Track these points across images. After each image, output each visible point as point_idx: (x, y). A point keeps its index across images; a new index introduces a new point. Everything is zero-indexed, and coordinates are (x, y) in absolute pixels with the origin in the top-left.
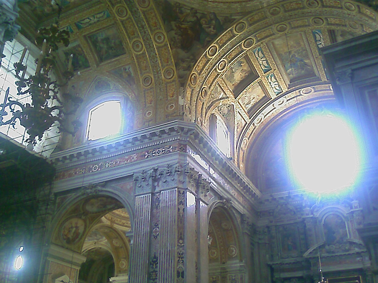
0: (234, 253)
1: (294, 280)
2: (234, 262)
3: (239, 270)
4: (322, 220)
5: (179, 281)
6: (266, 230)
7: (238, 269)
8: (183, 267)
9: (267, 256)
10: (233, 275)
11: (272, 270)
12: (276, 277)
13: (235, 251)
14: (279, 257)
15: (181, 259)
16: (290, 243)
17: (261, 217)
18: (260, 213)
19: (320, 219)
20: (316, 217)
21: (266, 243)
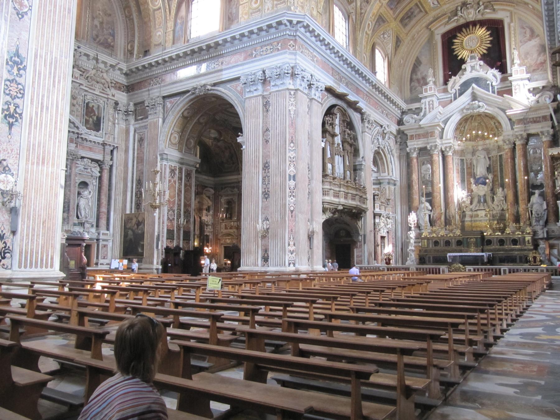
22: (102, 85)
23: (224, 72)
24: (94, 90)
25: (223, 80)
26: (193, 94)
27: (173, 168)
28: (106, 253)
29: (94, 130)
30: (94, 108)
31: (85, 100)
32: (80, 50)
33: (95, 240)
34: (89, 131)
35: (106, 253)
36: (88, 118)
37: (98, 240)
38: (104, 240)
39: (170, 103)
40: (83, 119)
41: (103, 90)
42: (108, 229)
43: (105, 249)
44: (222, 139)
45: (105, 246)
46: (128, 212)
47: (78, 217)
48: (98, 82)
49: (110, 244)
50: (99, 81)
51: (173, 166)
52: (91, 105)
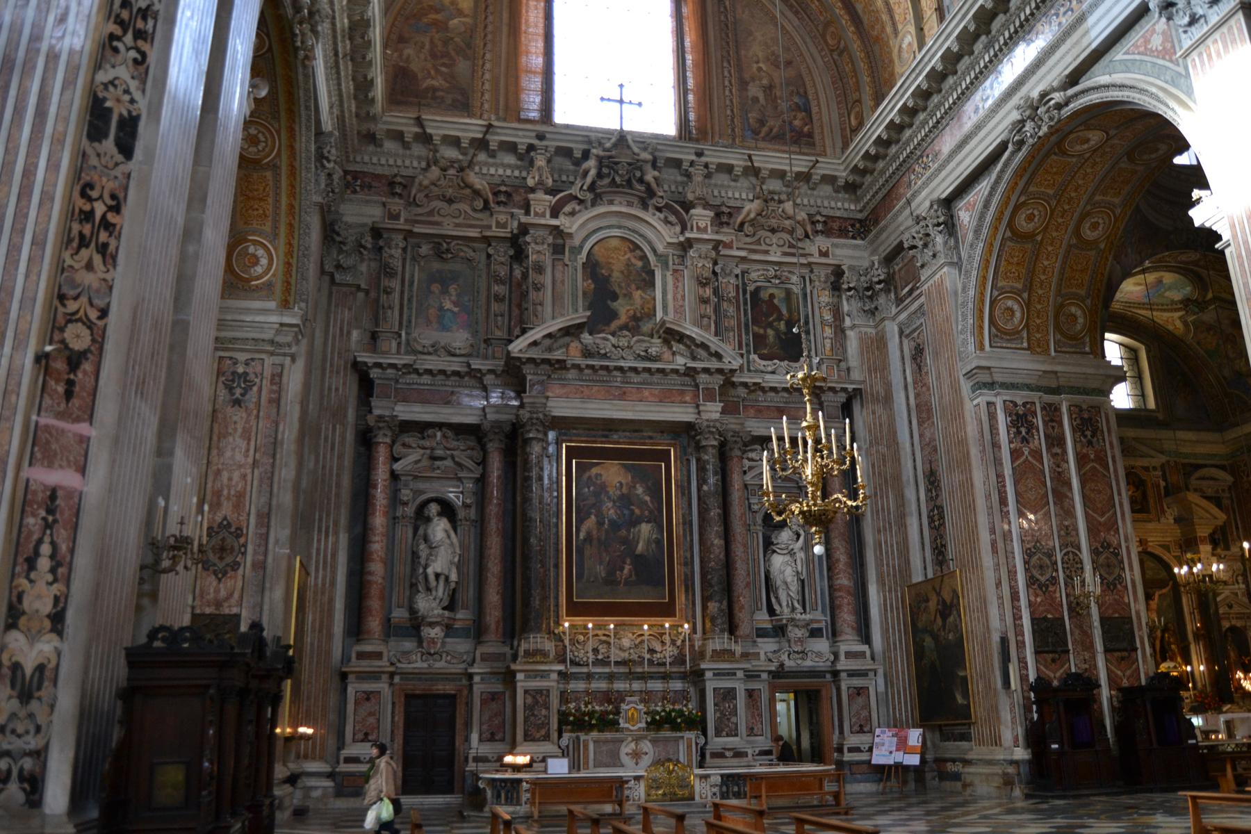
0: (259, 270)
1: (439, 434)
2: (257, 304)
3: (272, 342)
4: (581, 247)
5: (94, 161)
6: (368, 241)
7: (268, 335)
8: (137, 95)
9: (355, 334)
10: (241, 357)
11: (366, 386)
12: (377, 412)
13: (264, 261)
14: (399, 344)
15: (129, 38)
16: (448, 305)
17: (355, 192)
18: (355, 178)
19: (577, 242)
20: (569, 231)
21: (358, 287)
22: (786, 236)
23: (1091, 20)
24: (767, 252)
25: (1094, 46)
26: (1021, 143)
27: (1021, 410)
28: (864, 713)
29: (781, 360)
30: (776, 301)
31: (744, 284)
32: (704, 159)
33: (828, 676)
34: (770, 363)
35: (864, 713)
36: (762, 331)
37: (835, 674)
38: (852, 674)
39: (967, 209)
40: (747, 334)
41: (791, 246)
42: (866, 639)
43: (860, 700)
44: (1210, 295)
45: (860, 691)
46: (917, 577)
47: (771, 611)
48: (773, 231)
49: (877, 685)
50: (776, 226)
51: (1020, 402)
52: (764, 295)
